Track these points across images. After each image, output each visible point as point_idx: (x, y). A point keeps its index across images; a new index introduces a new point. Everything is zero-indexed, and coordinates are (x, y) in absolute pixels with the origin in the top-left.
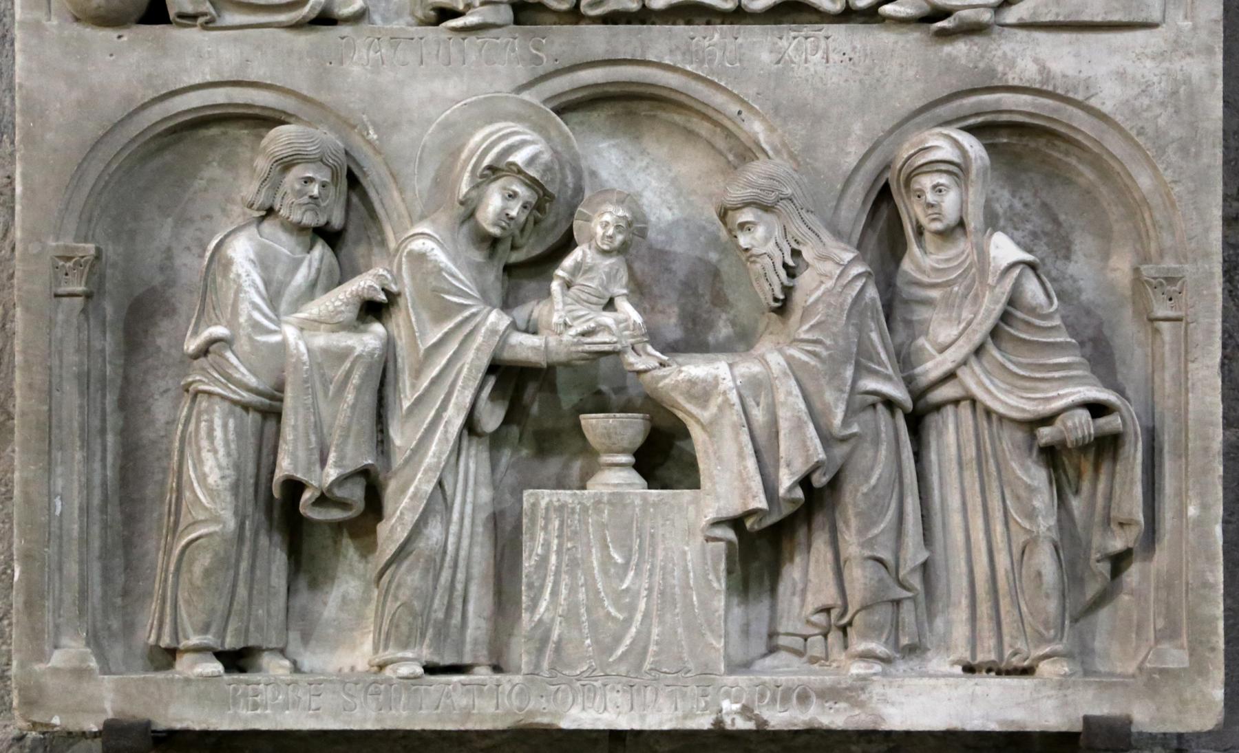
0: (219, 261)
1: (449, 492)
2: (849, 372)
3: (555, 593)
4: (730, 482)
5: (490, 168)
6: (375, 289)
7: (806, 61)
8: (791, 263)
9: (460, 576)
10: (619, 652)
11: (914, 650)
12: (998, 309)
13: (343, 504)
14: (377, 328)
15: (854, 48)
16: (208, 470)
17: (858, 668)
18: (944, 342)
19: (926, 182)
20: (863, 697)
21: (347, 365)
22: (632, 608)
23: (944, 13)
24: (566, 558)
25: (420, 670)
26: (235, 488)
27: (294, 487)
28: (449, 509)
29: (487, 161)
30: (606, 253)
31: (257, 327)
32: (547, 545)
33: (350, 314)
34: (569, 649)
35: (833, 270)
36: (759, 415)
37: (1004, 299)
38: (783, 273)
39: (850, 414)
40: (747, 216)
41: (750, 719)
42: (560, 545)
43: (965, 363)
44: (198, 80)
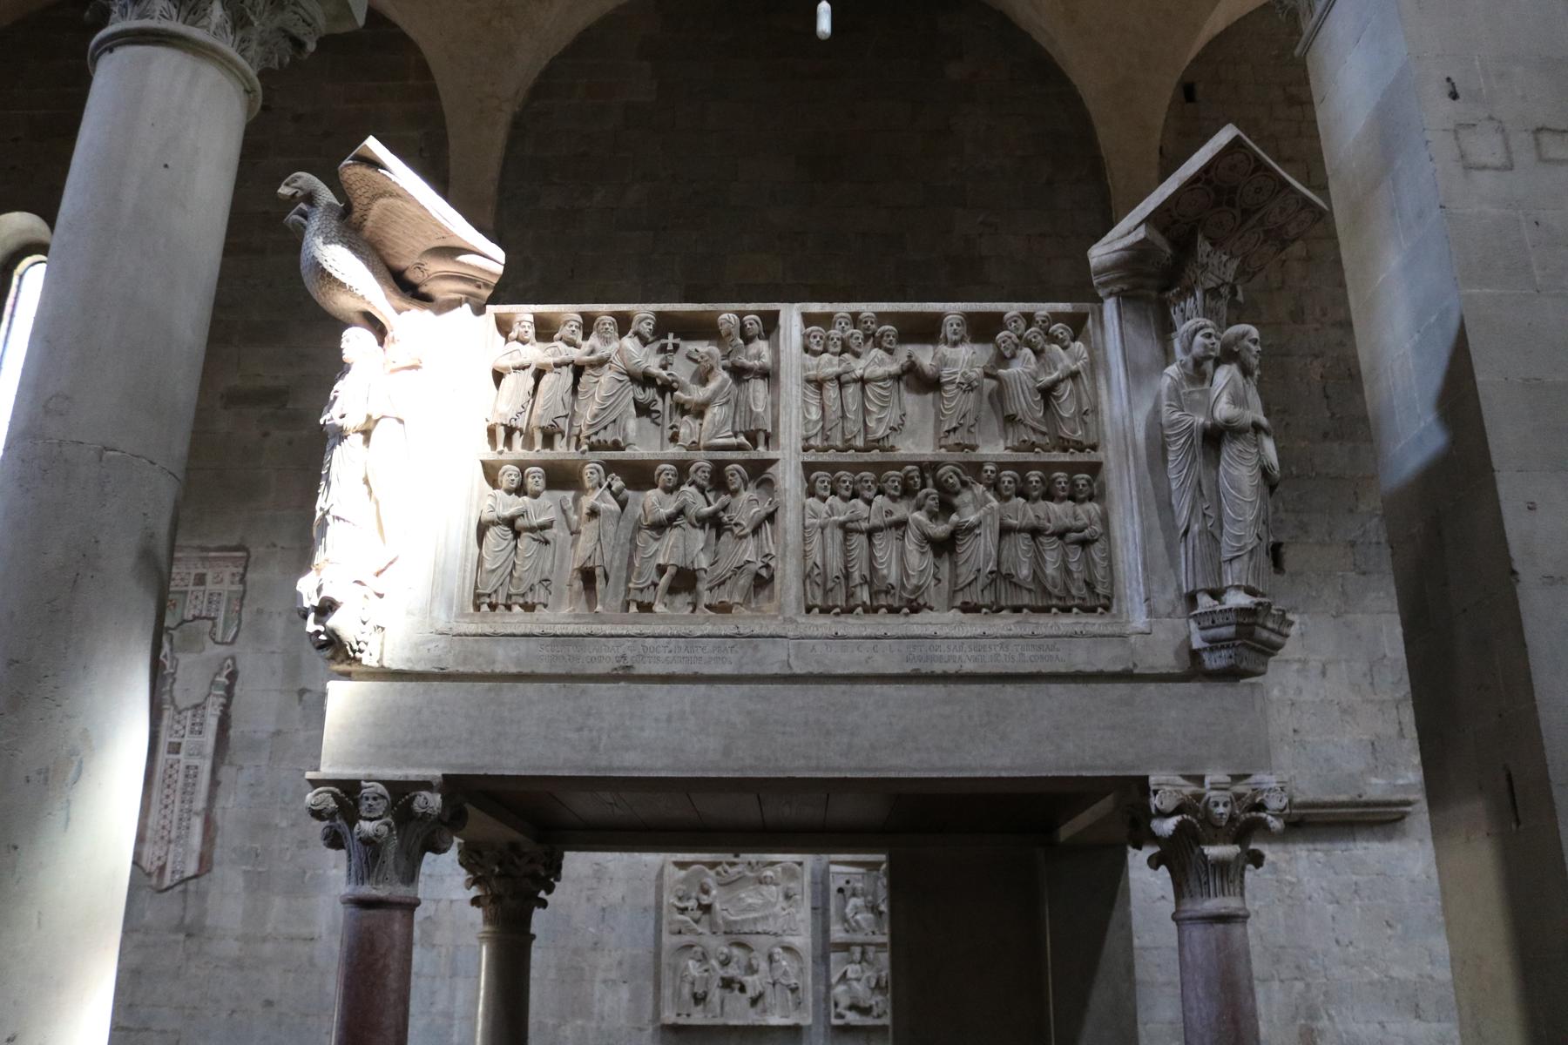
4: (750, 993)
16: (686, 991)
18: (778, 974)
35: (763, 966)
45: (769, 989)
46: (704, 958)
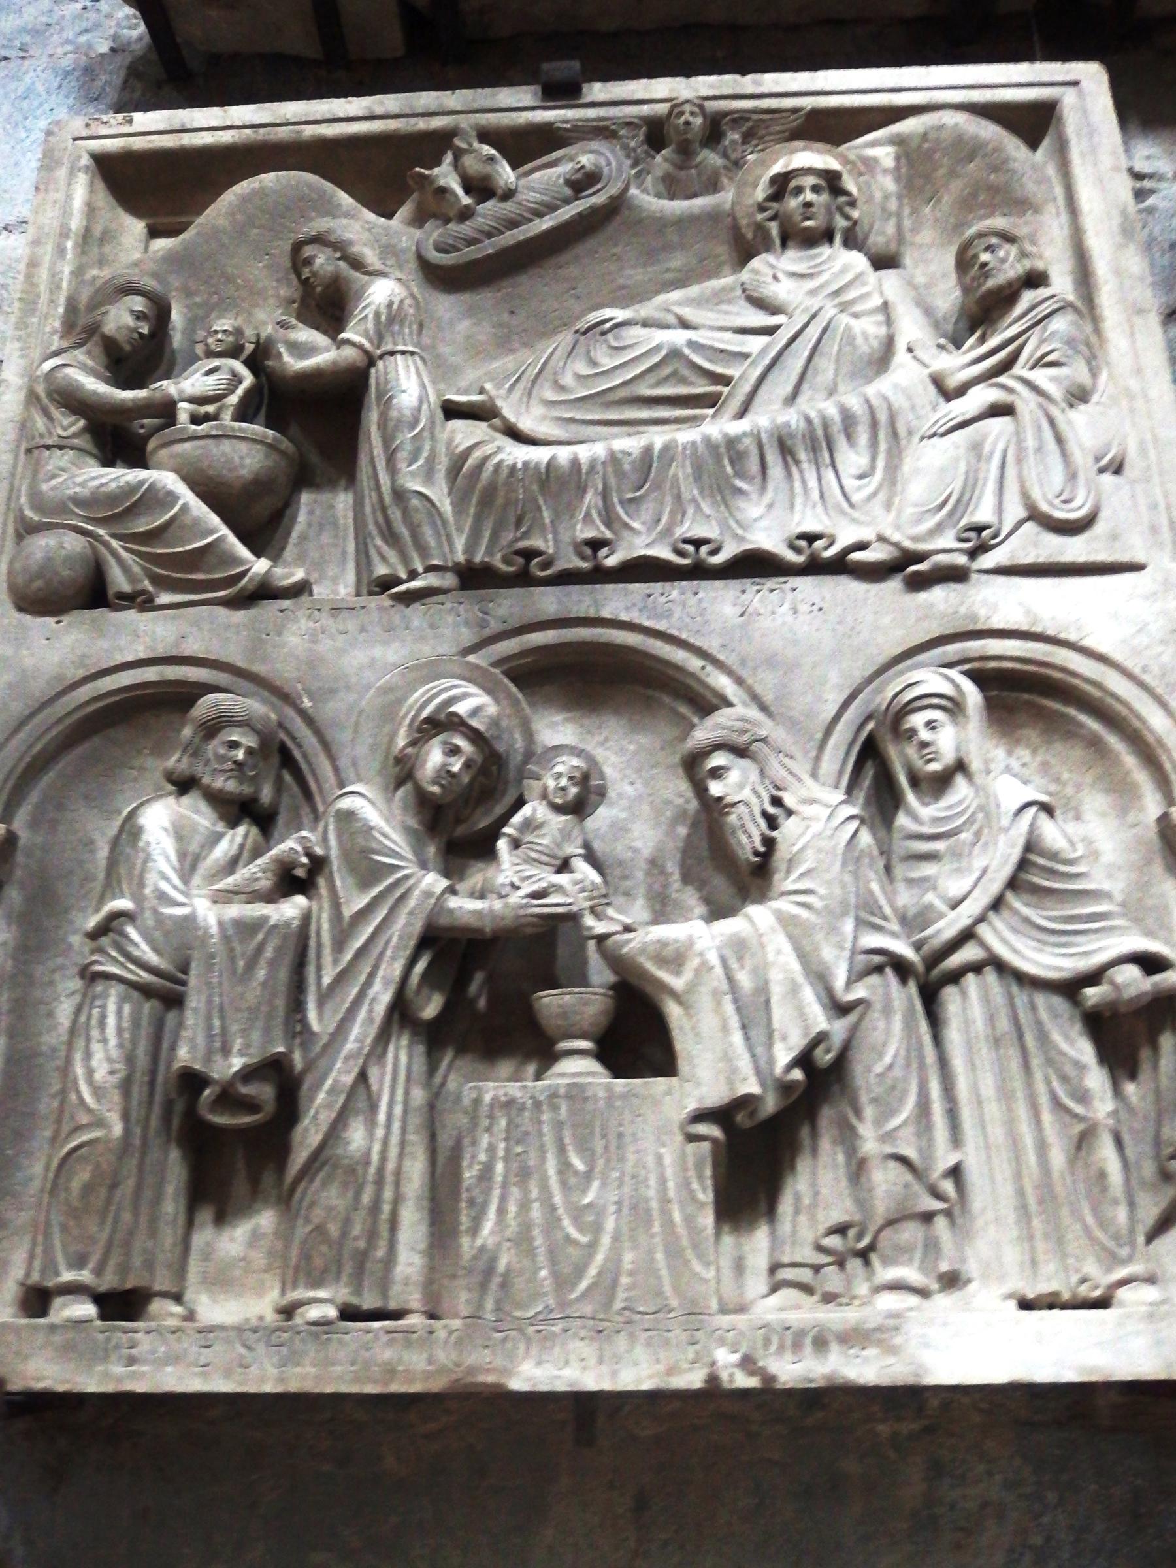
0: (130, 831)
1: (375, 1088)
2: (848, 926)
3: (501, 1211)
5: (427, 720)
6: (296, 852)
7: (773, 613)
8: (772, 810)
9: (388, 1194)
10: (583, 1285)
11: (952, 1281)
12: (1015, 854)
13: (250, 1106)
14: (300, 900)
15: (823, 599)
17: (889, 1301)
19: (917, 720)
20: (898, 1340)
21: (260, 936)
22: (596, 1229)
23: (920, 557)
24: (515, 1165)
25: (332, 1312)
26: (126, 1086)
27: (193, 1081)
28: (373, 1107)
29: (425, 714)
30: (559, 809)
31: (163, 897)
32: (491, 1149)
33: (265, 883)
34: (519, 1283)
35: (822, 820)
36: (744, 979)
37: (1021, 842)
38: (763, 823)
39: (857, 976)
40: (719, 759)
41: (752, 1373)
42: (507, 1150)
43: (981, 919)
44: (130, 657)
45: (890, 1032)
46: (268, 788)
